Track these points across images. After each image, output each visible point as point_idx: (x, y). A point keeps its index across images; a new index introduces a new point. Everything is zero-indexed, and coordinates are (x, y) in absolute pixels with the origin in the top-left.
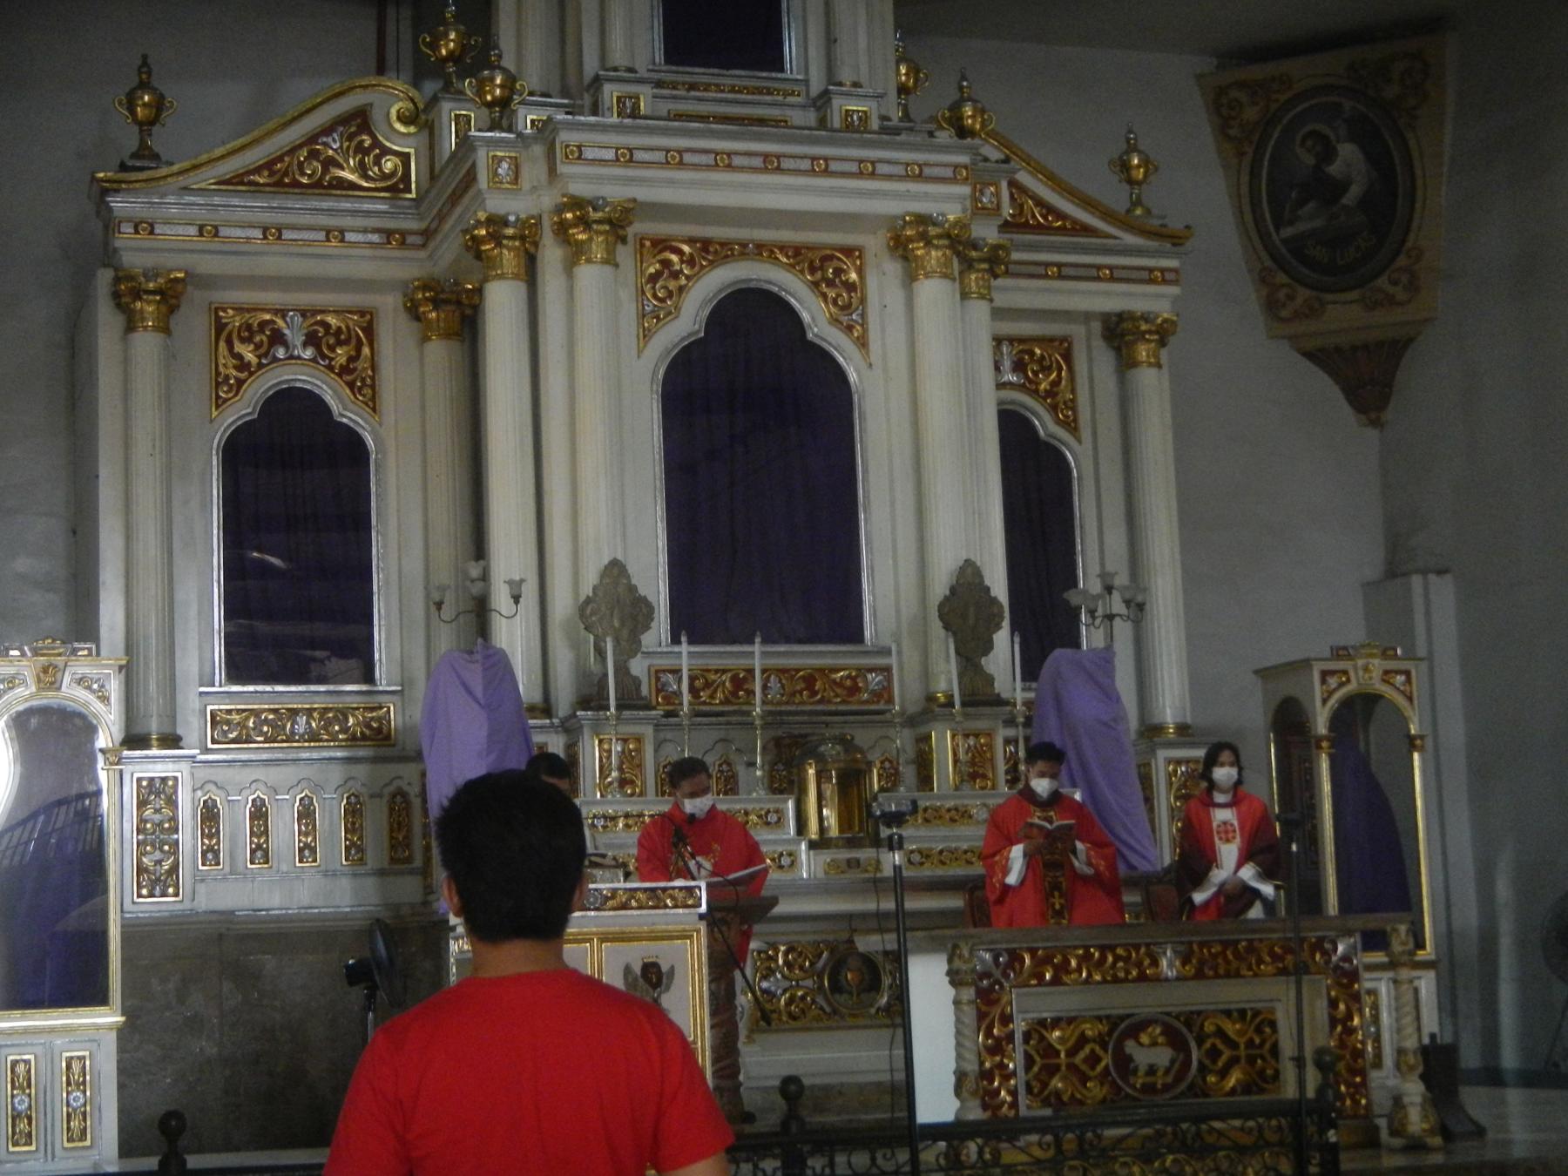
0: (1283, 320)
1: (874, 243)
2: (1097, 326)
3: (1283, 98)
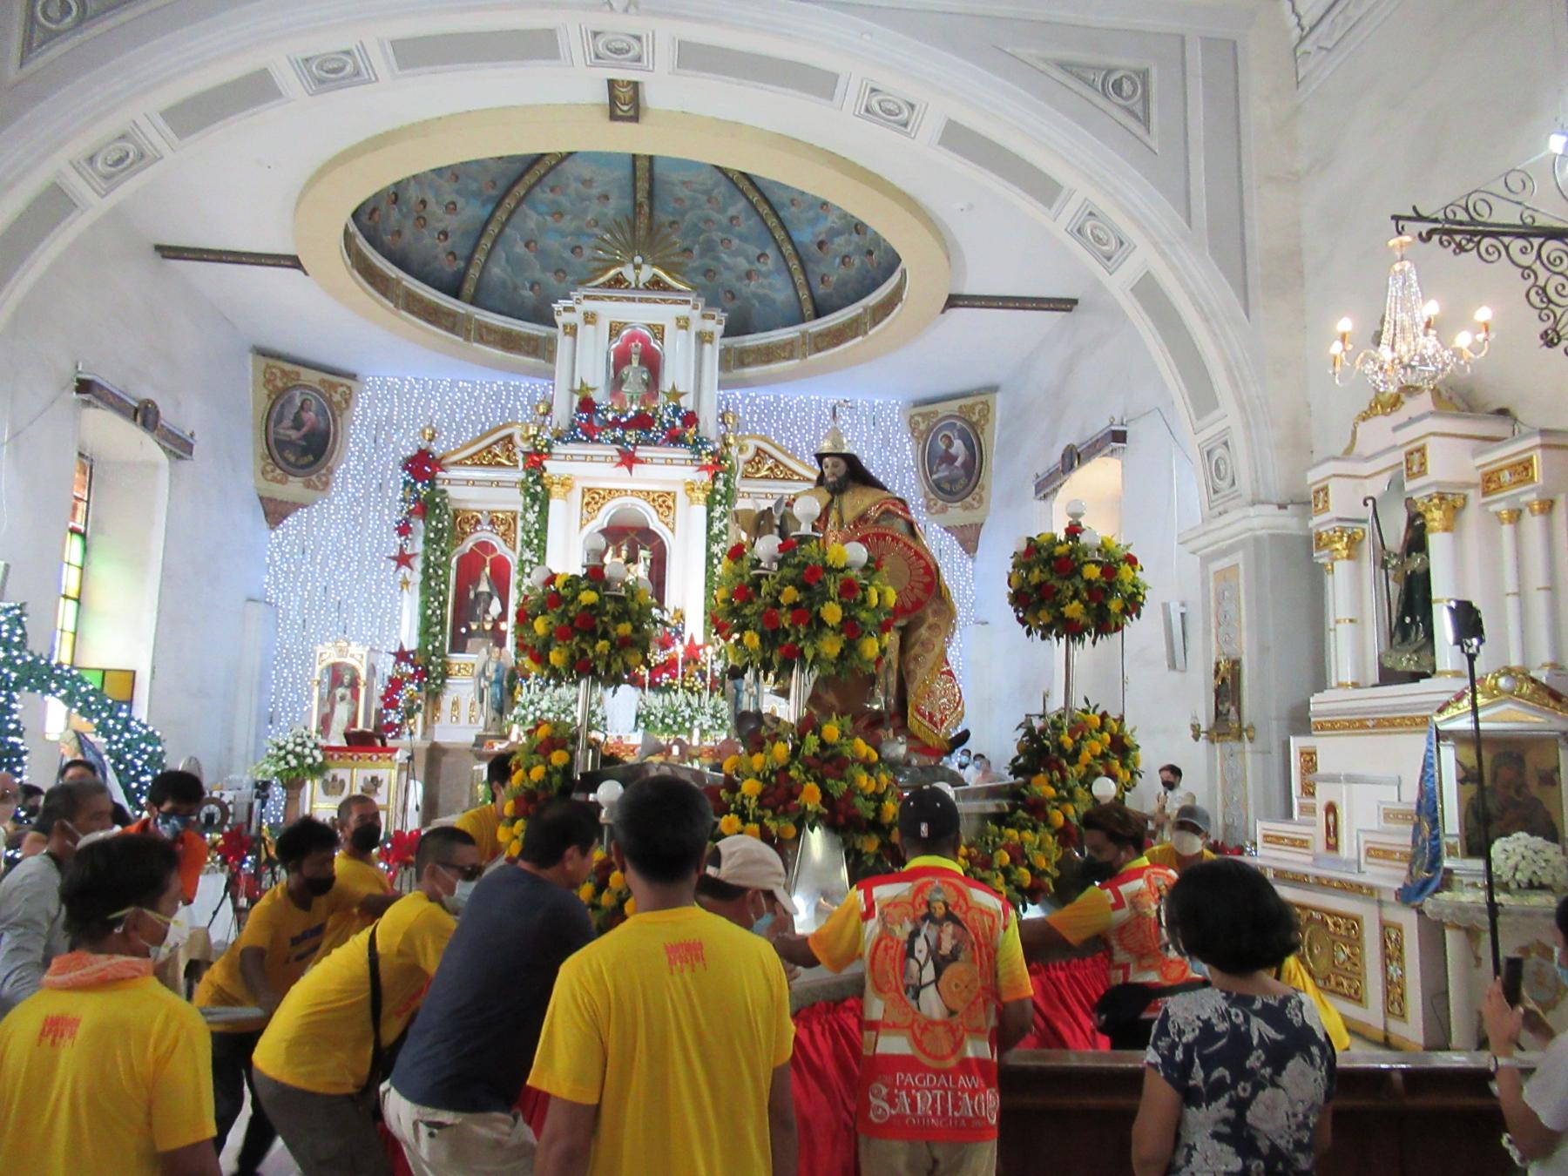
1: (680, 491)
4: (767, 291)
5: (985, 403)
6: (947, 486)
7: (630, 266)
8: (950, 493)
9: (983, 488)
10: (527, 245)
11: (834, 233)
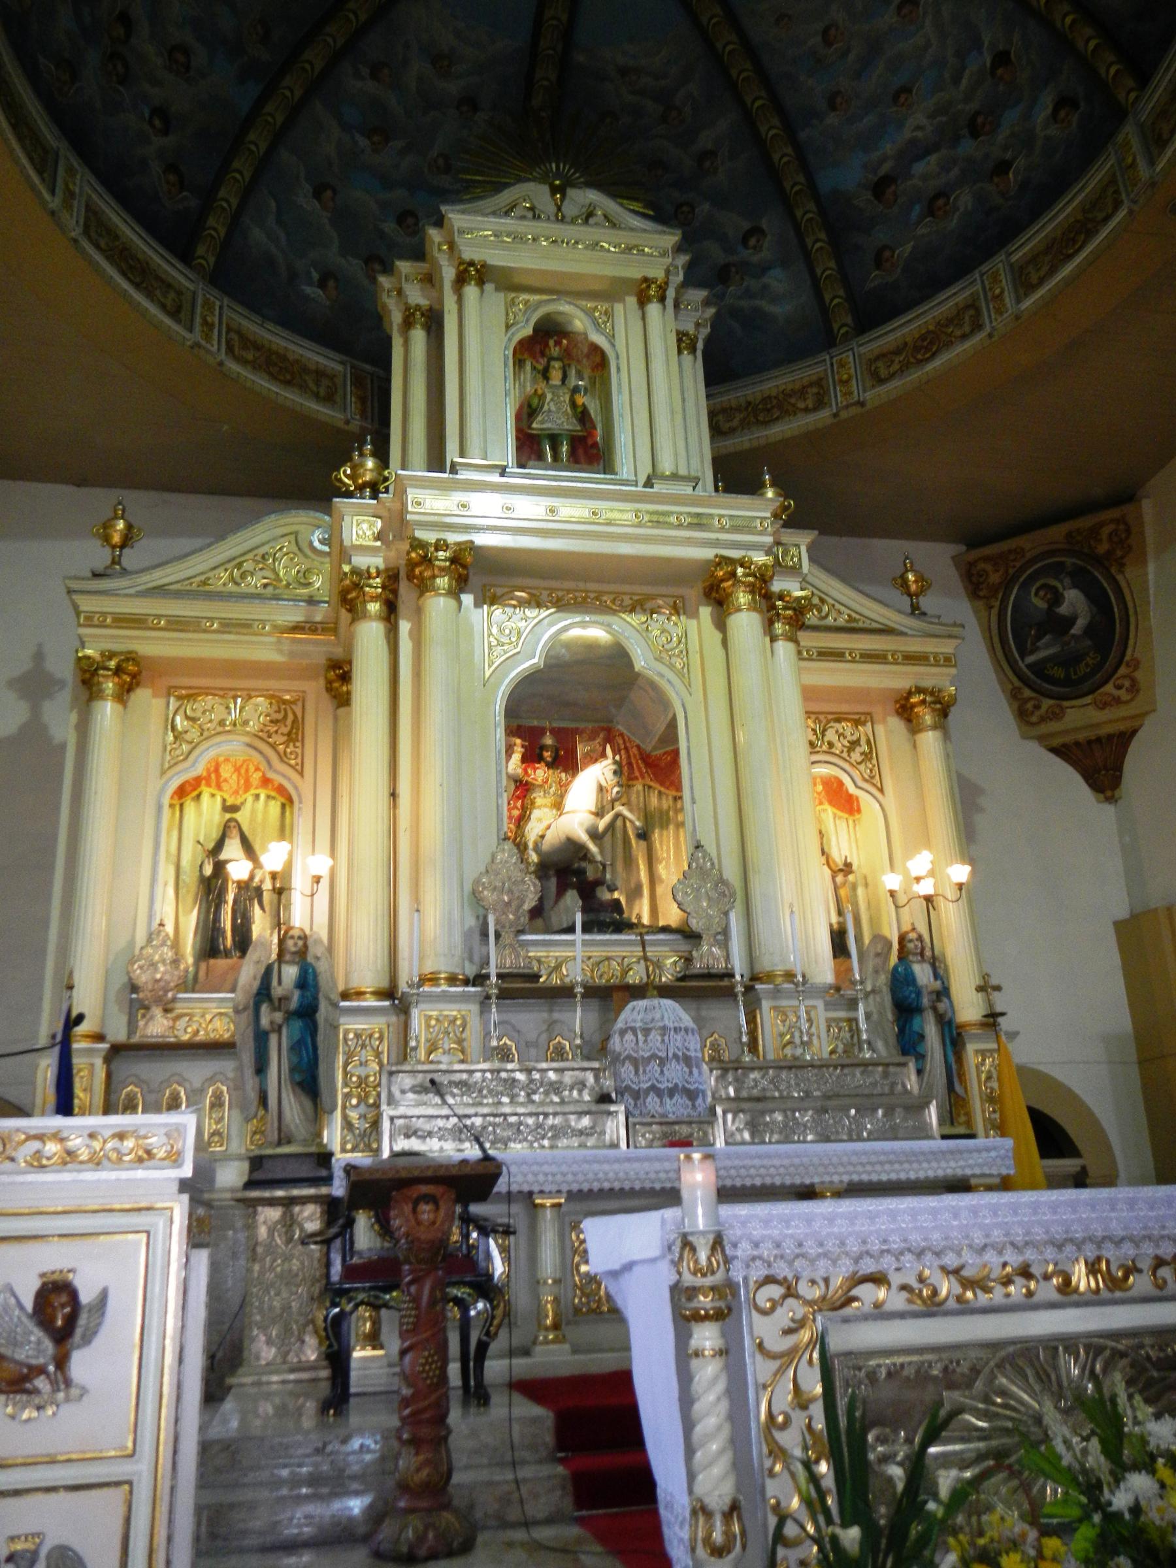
0: (1033, 724)
2: (891, 707)
3: (1018, 565)
4: (758, 302)
5: (1117, 521)
6: (1059, 673)
7: (545, 189)
8: (1067, 682)
9: (1136, 664)
10: (317, 194)
11: (916, 151)
